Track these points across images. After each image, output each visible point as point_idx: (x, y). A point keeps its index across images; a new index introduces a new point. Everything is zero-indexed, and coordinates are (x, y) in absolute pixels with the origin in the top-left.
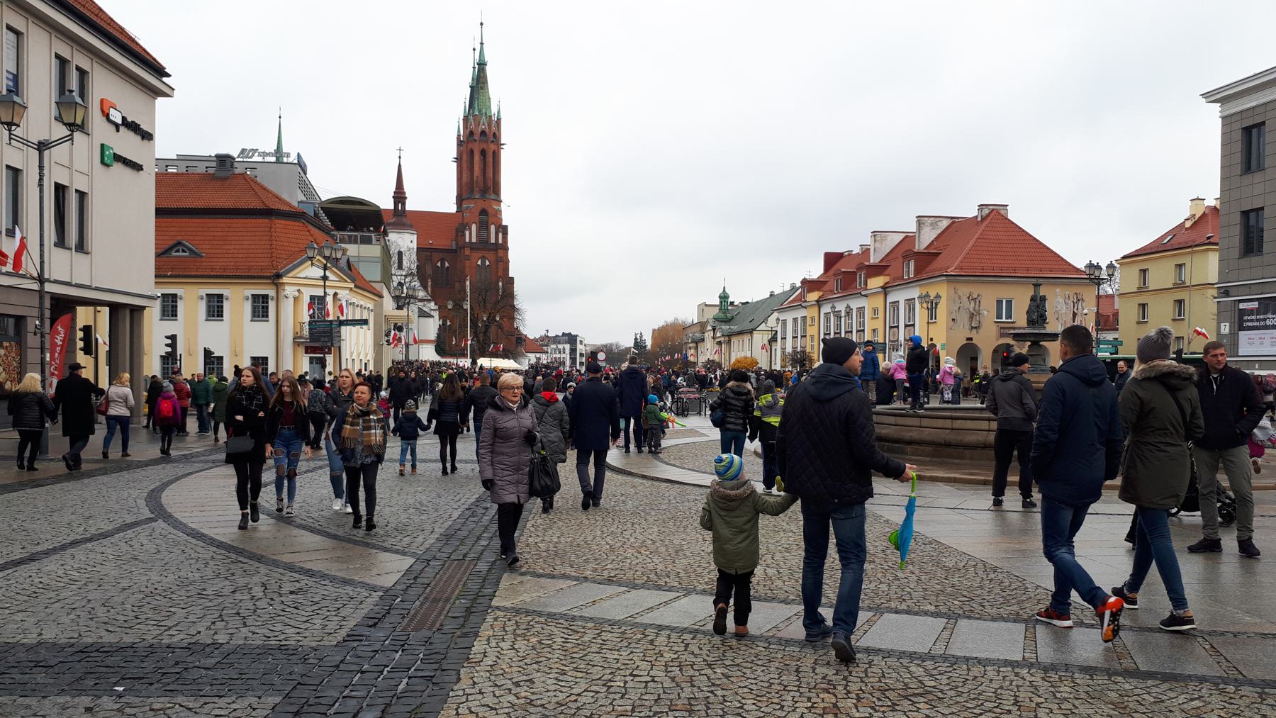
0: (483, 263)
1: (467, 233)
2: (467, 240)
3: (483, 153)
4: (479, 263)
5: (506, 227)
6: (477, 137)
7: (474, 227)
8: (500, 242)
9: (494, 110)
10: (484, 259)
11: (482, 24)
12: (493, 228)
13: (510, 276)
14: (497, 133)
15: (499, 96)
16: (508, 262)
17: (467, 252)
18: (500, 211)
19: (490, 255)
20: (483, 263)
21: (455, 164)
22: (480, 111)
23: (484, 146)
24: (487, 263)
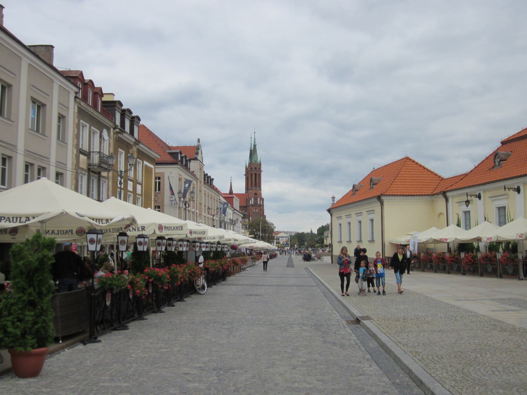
0: (256, 211)
1: (250, 201)
2: (251, 203)
3: (256, 174)
4: (254, 211)
7: (253, 199)
8: (261, 204)
9: (259, 160)
10: (256, 209)
11: (255, 132)
12: (259, 199)
15: (260, 155)
16: (264, 210)
17: (251, 207)
18: (261, 193)
19: (258, 208)
20: (256, 211)
23: (256, 172)
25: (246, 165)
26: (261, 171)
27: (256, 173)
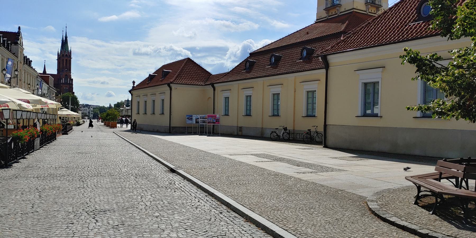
1: (62, 80)
2: (62, 82)
3: (66, 60)
4: (65, 88)
5: (72, 79)
6: (65, 56)
7: (63, 79)
8: (71, 83)
9: (69, 49)
10: (66, 87)
13: (73, 91)
14: (70, 55)
15: (71, 46)
17: (62, 85)
21: (57, 61)
22: (66, 49)
24: (67, 88)
25: (58, 52)
26: (71, 58)
27: (67, 59)
